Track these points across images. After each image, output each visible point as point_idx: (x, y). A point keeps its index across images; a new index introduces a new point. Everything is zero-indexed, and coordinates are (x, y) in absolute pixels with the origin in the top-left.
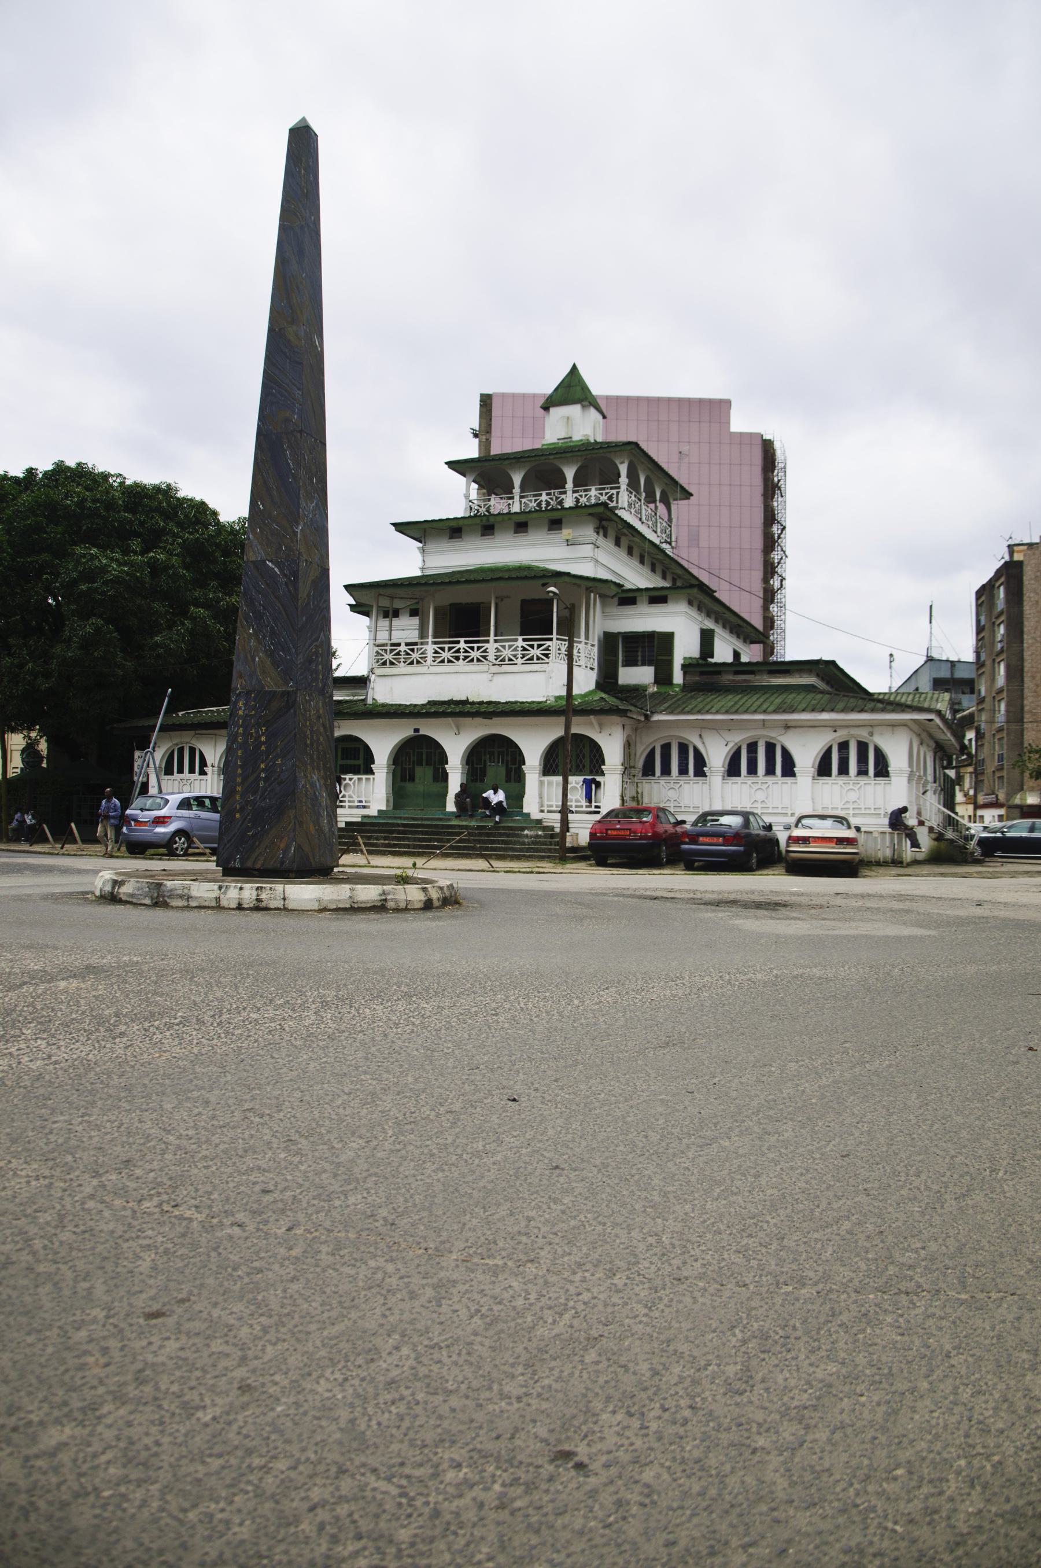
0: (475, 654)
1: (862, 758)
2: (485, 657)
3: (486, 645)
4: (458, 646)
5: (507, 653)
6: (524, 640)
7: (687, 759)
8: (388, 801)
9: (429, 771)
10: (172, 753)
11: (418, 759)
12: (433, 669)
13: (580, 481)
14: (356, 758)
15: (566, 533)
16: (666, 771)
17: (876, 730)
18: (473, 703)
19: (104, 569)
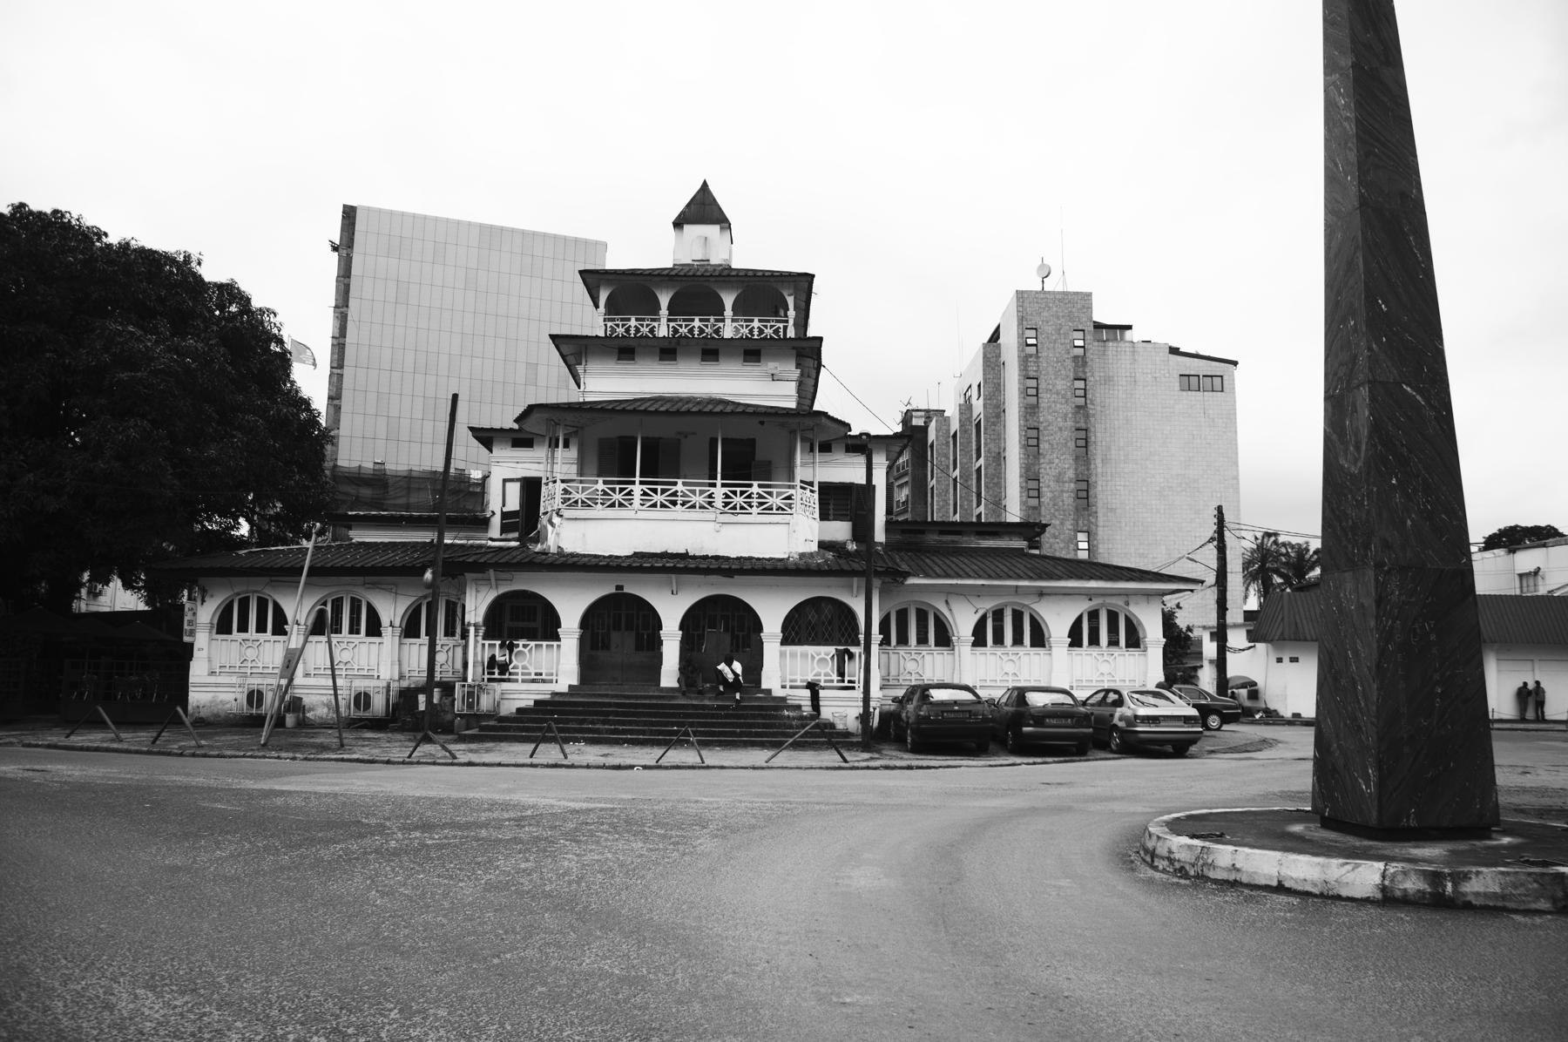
4: (674, 489)
5: (739, 500)
7: (926, 627)
9: (630, 639)
10: (231, 603)
12: (641, 515)
13: (741, 309)
15: (771, 366)
17: (1132, 600)
18: (694, 557)
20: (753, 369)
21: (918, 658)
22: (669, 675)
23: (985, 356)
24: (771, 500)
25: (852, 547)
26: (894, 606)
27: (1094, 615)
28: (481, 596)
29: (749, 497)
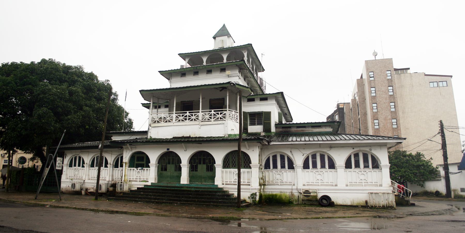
0: (193, 117)
2: (197, 119)
3: (198, 114)
4: (186, 114)
6: (214, 111)
7: (284, 161)
8: (155, 179)
11: (169, 162)
12: (175, 124)
14: (143, 161)
16: (275, 167)
18: (192, 138)
21: (281, 173)
22: (184, 179)
24: (218, 116)
26: (268, 154)
28: (127, 153)
29: (211, 115)
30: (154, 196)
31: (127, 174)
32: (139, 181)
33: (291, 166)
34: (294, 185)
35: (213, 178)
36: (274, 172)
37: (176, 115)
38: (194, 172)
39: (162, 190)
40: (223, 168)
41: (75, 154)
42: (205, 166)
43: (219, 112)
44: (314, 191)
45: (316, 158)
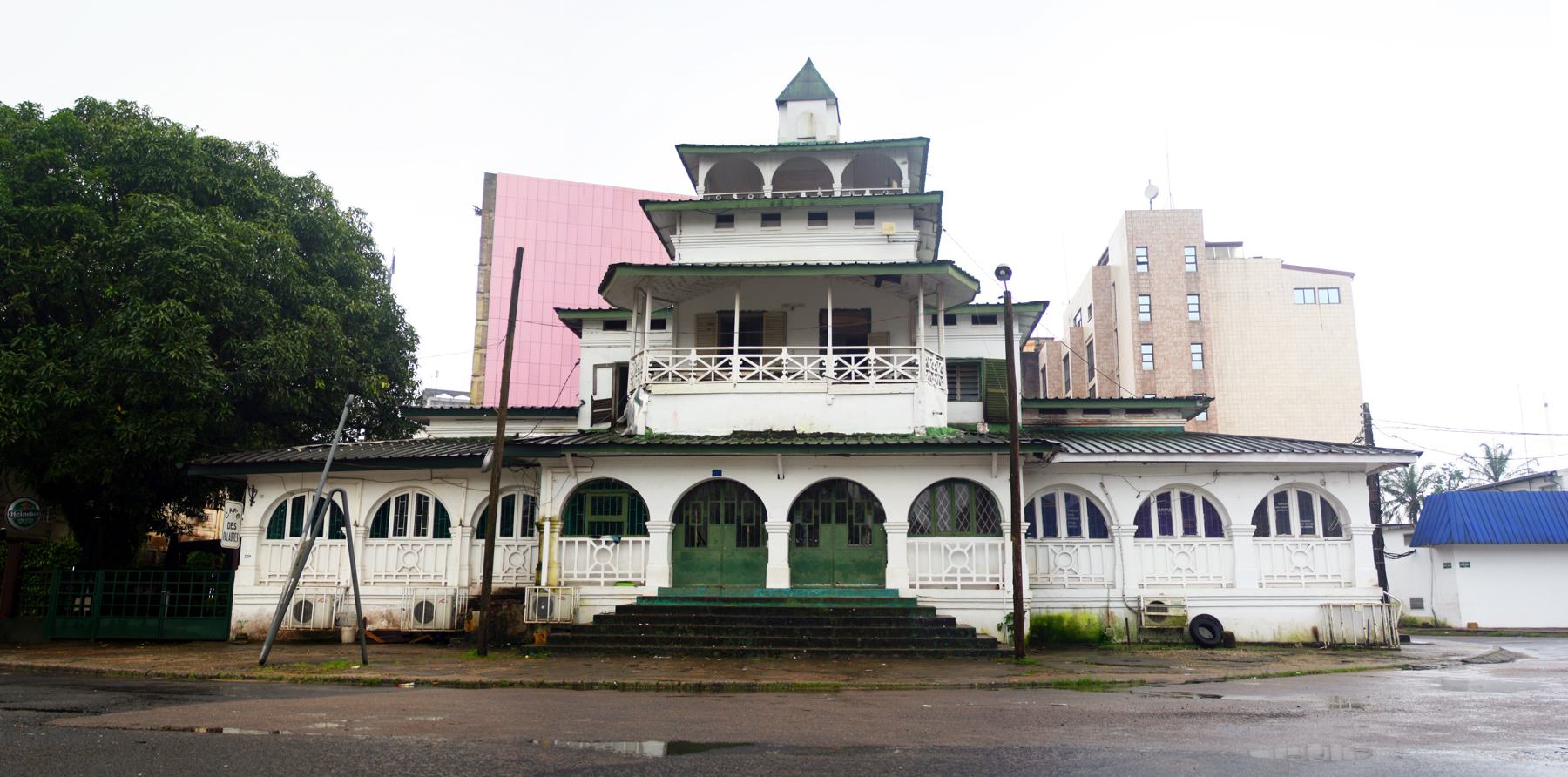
1: (1306, 513)
2: (821, 373)
4: (778, 357)
6: (878, 351)
7: (1078, 515)
11: (719, 513)
12: (740, 388)
14: (616, 510)
15: (885, 226)
17: (1328, 478)
18: (803, 436)
19: (187, 232)
20: (865, 231)
22: (778, 576)
23: (1094, 279)
24: (891, 367)
25: (984, 429)
27: (1281, 498)
28: (557, 486)
29: (865, 364)
30: (697, 631)
31: (555, 558)
32: (606, 584)
33: (1100, 529)
34: (1113, 586)
35: (877, 567)
36: (1051, 546)
37: (744, 356)
38: (807, 550)
39: (715, 610)
40: (909, 535)
41: (298, 487)
42: (843, 529)
43: (853, 356)
44: (1177, 601)
45: (1169, 505)
